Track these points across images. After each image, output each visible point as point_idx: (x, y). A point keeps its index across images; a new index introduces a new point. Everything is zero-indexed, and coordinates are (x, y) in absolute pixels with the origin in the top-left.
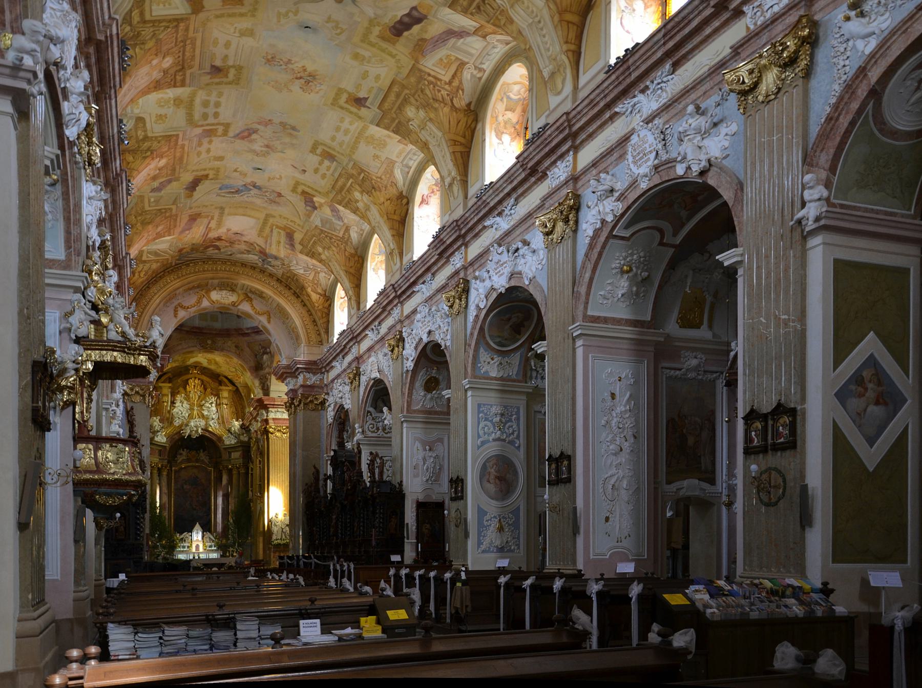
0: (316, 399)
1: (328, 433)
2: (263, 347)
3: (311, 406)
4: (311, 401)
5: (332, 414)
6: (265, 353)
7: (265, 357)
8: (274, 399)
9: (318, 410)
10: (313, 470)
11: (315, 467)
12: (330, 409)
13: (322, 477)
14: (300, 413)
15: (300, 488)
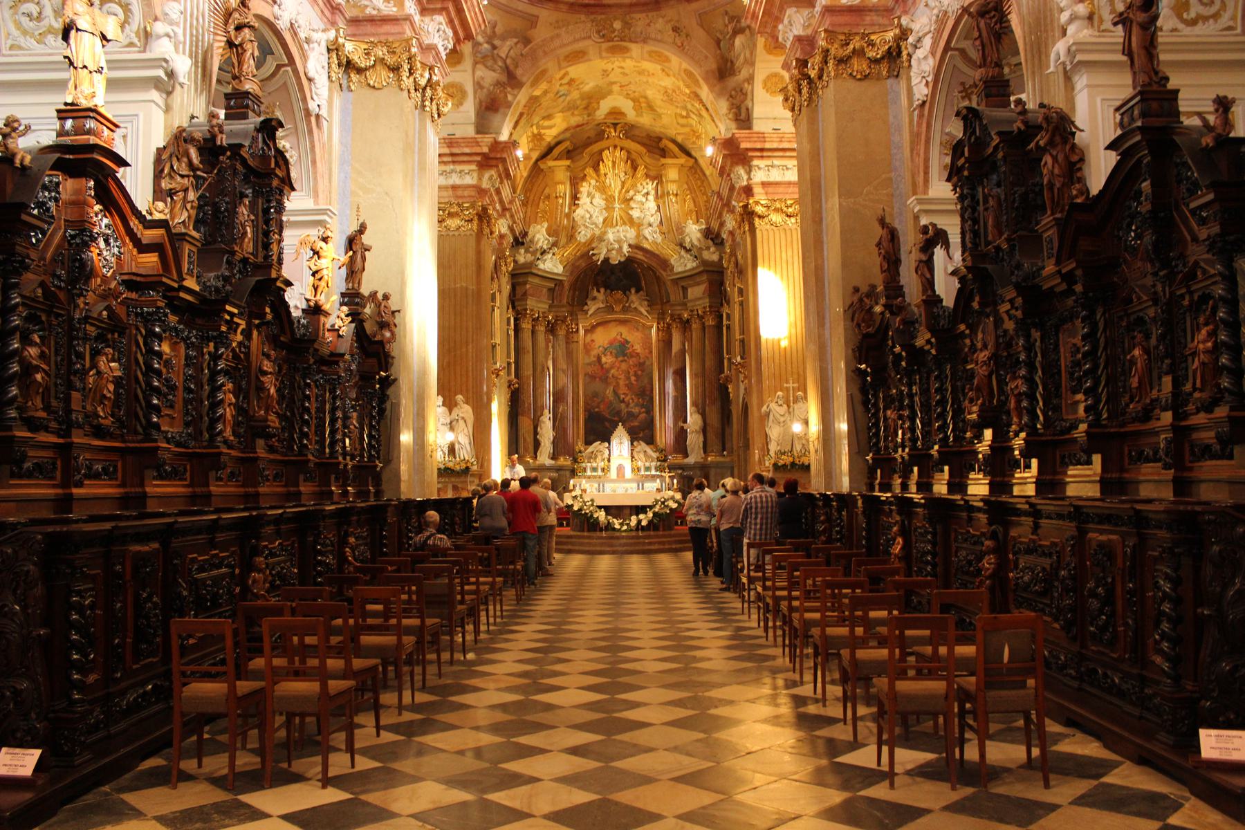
0: (871, 44)
1: (915, 137)
2: (732, 18)
3: (858, 65)
4: (859, 53)
5: (929, 65)
6: (737, 31)
7: (739, 41)
8: (762, 136)
9: (879, 78)
10: (879, 232)
11: (882, 222)
12: (920, 53)
13: (909, 242)
14: (832, 93)
15: (836, 306)
